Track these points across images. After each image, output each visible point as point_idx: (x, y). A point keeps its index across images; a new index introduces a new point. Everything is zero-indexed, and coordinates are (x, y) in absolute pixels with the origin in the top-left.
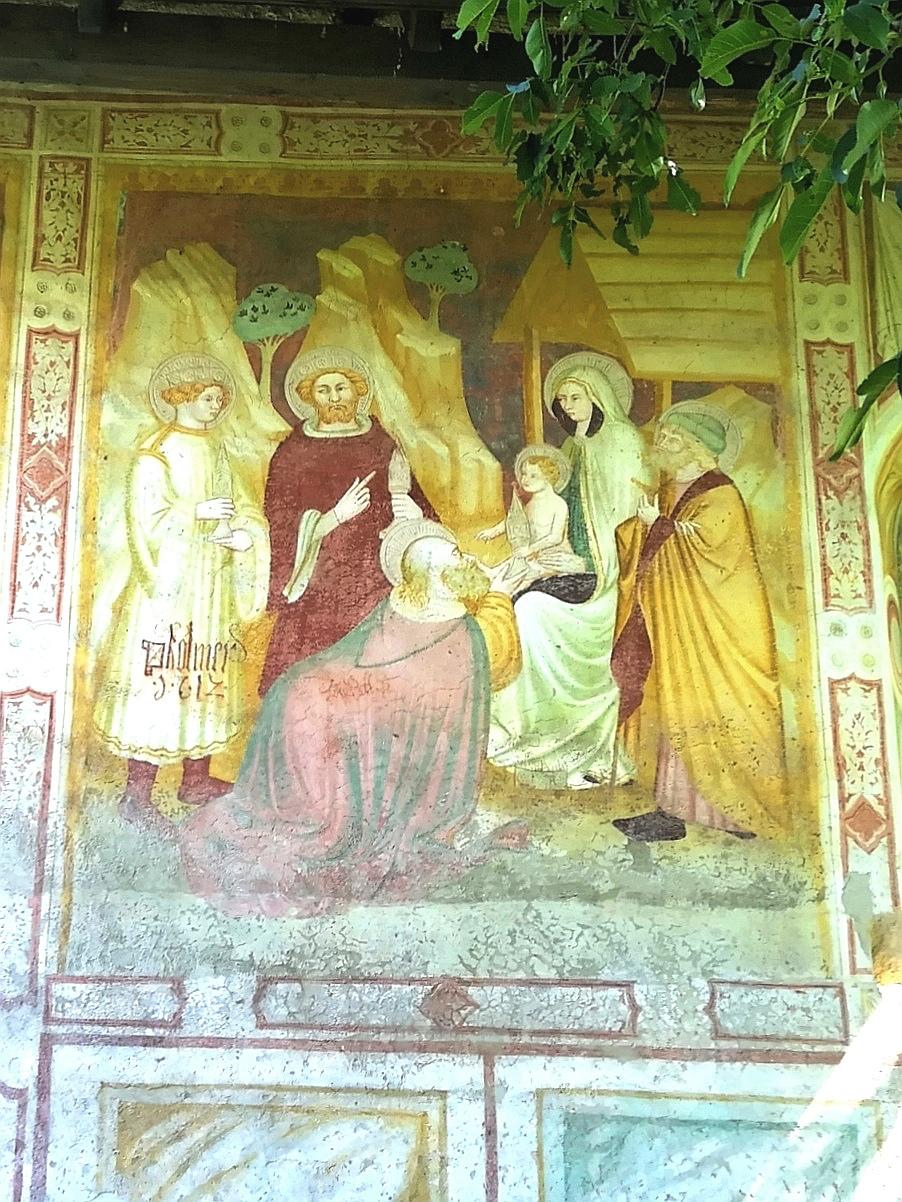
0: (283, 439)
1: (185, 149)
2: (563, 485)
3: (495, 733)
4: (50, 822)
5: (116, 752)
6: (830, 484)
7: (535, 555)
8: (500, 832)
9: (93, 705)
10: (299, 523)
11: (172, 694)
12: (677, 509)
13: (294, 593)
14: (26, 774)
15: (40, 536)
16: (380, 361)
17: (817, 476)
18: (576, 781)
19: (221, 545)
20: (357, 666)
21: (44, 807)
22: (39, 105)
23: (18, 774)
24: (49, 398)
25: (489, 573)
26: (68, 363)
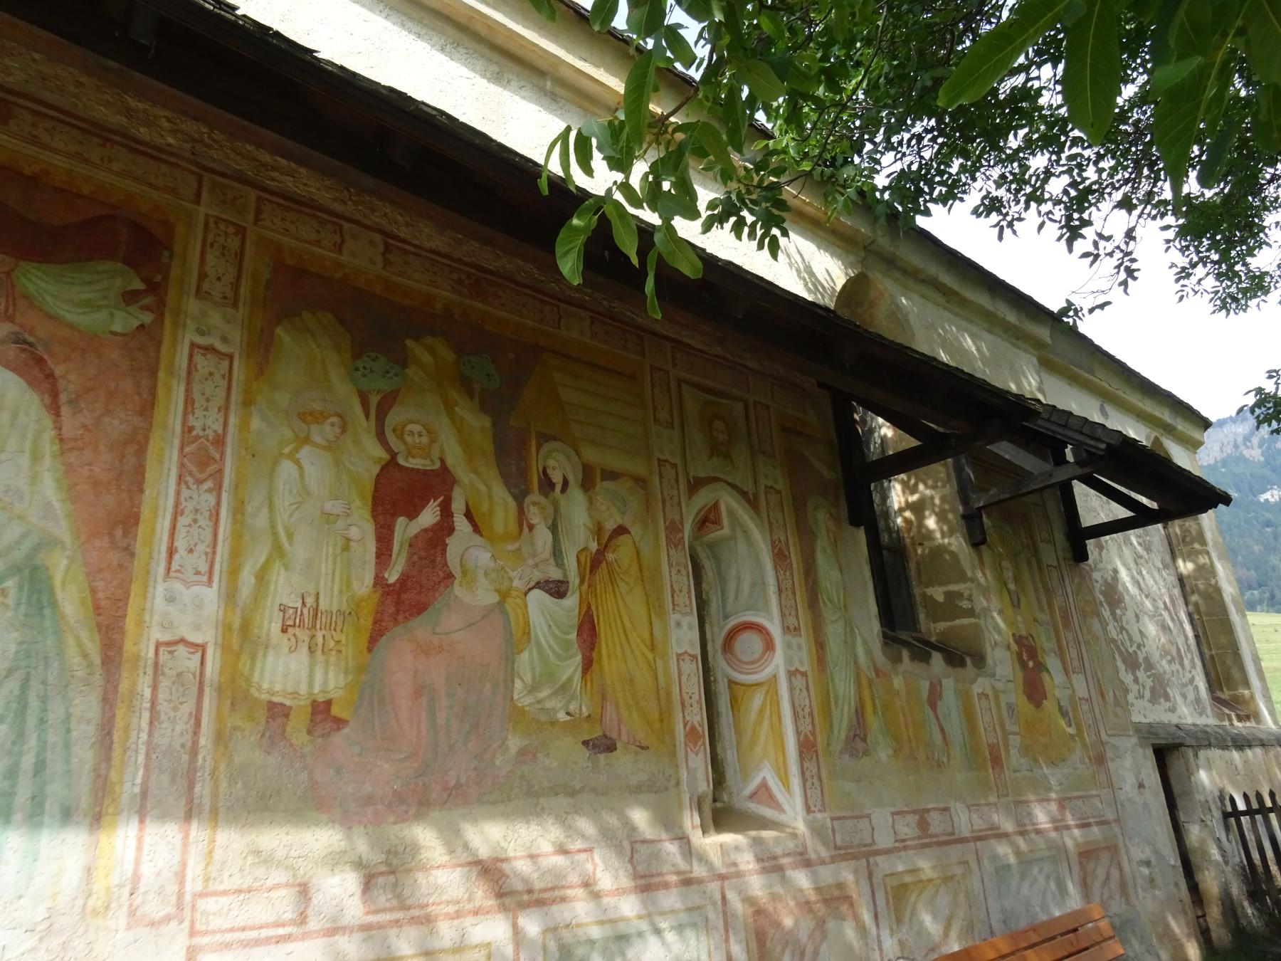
0: (383, 463)
1: (317, 243)
2: (550, 523)
3: (518, 684)
4: (200, 757)
5: (256, 694)
7: (536, 565)
8: (522, 752)
9: (239, 655)
10: (395, 525)
11: (305, 650)
12: (606, 546)
13: (393, 577)
14: (179, 714)
15: (196, 511)
16: (446, 421)
18: (562, 716)
19: (340, 534)
20: (435, 633)
21: (195, 743)
22: (207, 177)
23: (172, 714)
24: (208, 400)
25: (512, 574)
26: (223, 376)
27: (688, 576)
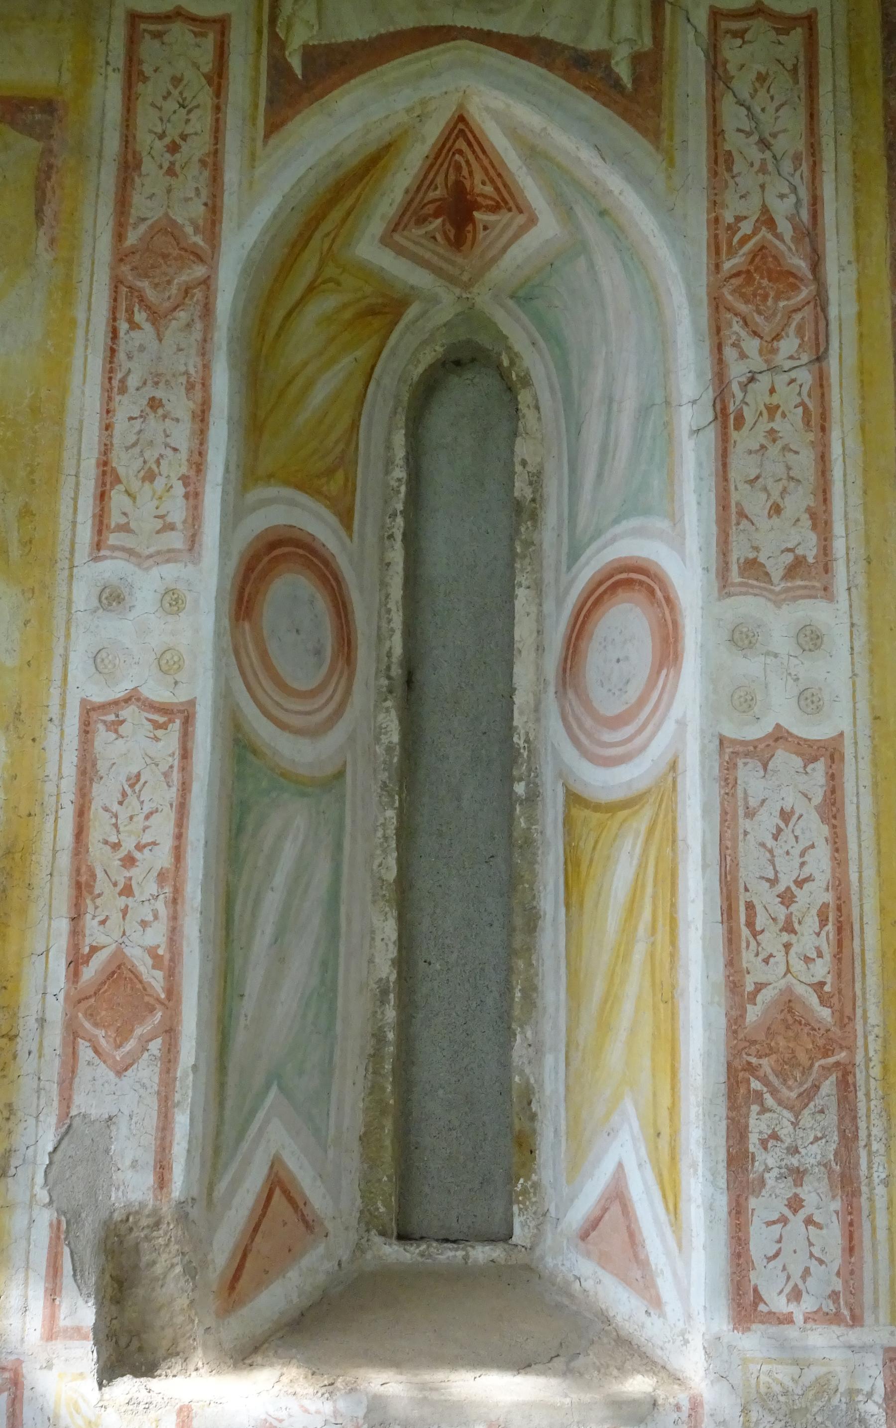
6: (142, 300)
17: (117, 283)
27: (202, 416)
